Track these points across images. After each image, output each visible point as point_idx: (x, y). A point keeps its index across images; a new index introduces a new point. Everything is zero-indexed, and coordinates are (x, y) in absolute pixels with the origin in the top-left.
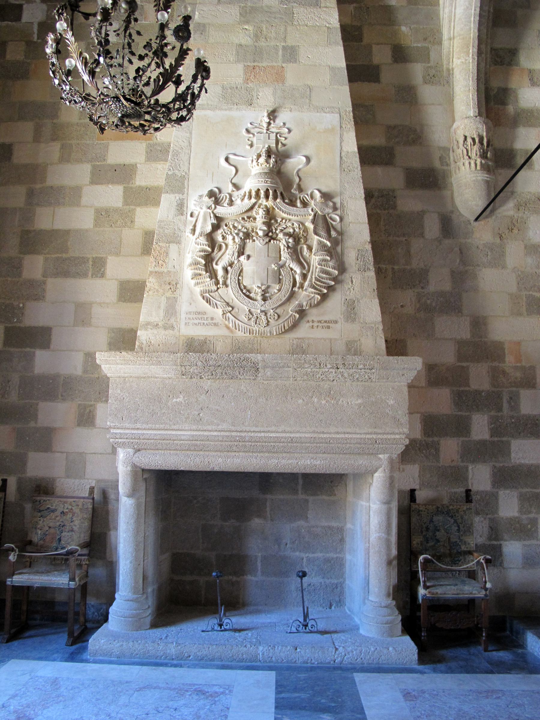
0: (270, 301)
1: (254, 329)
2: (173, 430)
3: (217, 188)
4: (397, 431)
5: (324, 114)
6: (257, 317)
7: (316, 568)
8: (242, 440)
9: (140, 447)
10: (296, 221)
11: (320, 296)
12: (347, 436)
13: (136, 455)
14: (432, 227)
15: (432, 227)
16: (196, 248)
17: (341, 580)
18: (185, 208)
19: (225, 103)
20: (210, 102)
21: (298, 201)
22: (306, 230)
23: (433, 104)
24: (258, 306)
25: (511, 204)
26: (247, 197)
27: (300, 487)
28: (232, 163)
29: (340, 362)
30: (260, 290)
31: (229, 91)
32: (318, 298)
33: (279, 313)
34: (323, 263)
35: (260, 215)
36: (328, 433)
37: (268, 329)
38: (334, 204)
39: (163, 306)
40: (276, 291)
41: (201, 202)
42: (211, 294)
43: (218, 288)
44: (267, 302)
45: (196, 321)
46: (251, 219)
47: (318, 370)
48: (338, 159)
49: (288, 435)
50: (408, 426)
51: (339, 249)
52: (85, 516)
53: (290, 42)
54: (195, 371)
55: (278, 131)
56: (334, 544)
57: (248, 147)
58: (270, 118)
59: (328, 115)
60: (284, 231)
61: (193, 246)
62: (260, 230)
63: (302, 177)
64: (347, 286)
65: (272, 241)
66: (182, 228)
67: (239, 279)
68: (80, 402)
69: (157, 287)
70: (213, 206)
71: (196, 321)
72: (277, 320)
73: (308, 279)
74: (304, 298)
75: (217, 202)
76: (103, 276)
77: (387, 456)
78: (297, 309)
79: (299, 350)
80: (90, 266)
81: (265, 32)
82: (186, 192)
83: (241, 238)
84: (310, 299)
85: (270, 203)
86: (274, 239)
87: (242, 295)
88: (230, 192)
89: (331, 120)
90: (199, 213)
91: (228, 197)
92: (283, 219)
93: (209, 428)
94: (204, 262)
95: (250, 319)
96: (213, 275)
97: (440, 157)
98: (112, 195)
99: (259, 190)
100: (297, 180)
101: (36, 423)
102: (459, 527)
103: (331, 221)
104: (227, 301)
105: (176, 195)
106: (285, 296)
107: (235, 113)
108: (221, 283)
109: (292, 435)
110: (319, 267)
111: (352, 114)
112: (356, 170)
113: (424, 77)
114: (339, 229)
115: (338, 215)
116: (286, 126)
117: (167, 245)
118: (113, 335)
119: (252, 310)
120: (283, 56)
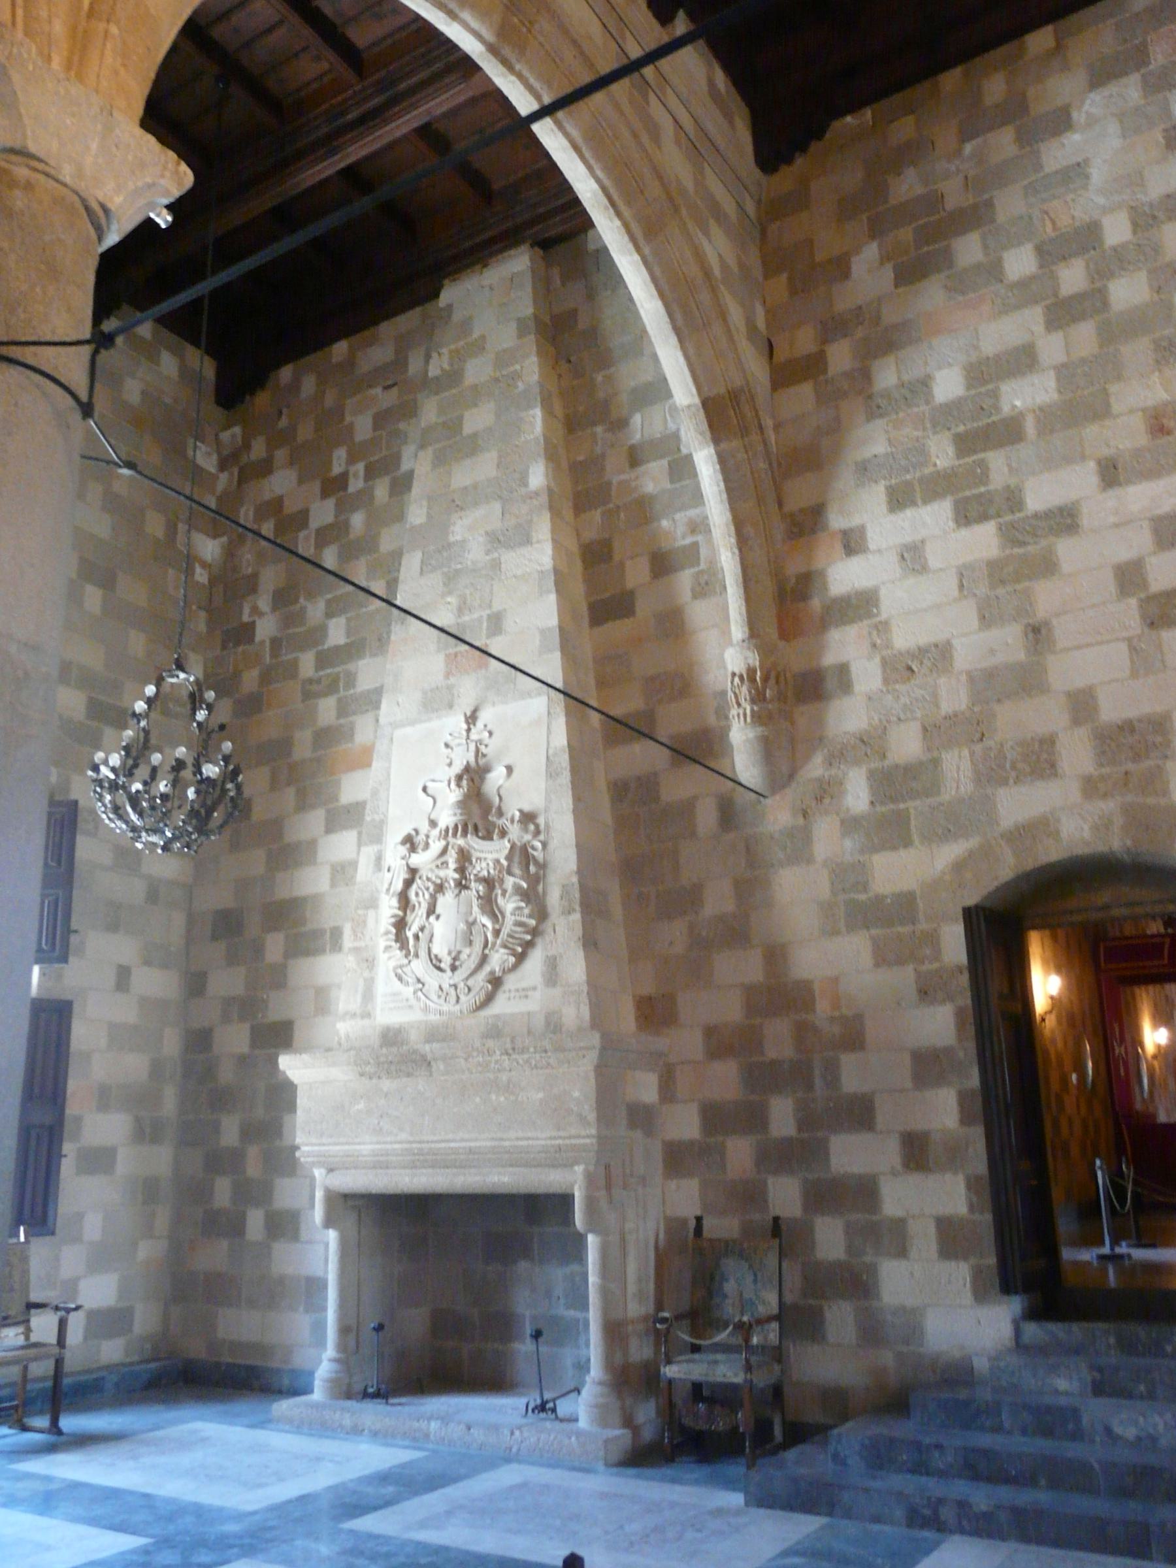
8: (421, 1152)
14: (707, 817)
15: (707, 817)
24: (447, 979)
25: (818, 759)
29: (509, 1046)
35: (452, 859)
37: (458, 1007)
44: (456, 973)
45: (392, 1005)
48: (544, 760)
51: (540, 888)
53: (496, 607)
64: (549, 936)
75: (413, 849)
79: (494, 1031)
81: (469, 601)
85: (461, 842)
95: (439, 997)
100: (497, 799)
102: (755, 1275)
107: (435, 724)
109: (472, 1144)
113: (693, 590)
120: (488, 629)
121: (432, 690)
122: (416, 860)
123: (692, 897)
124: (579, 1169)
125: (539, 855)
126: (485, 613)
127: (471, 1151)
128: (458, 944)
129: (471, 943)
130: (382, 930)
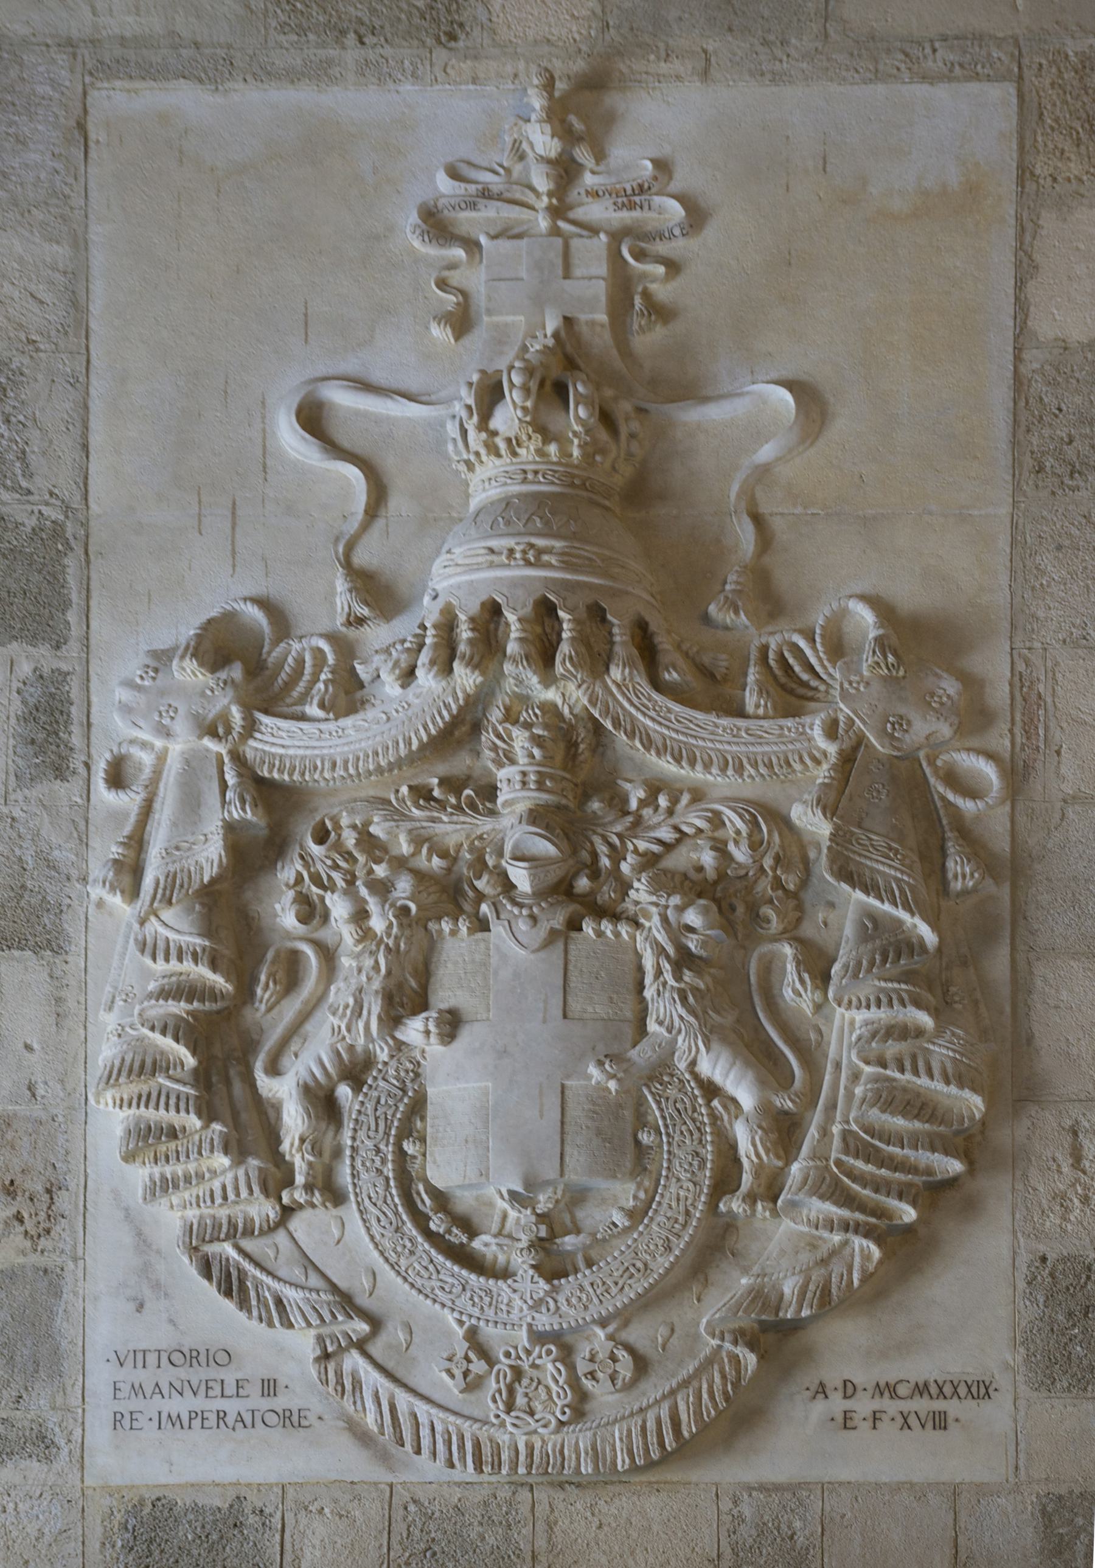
0: (585, 1276)
1: (503, 1439)
5: (921, 90)
11: (879, 1242)
18: (75, 729)
19: (283, 28)
22: (794, 852)
24: (517, 1308)
28: (345, 443)
32: (866, 1257)
34: (892, 1048)
37: (581, 1438)
38: (971, 683)
40: (619, 1218)
41: (162, 693)
42: (247, 1244)
43: (288, 1211)
46: (468, 792)
55: (626, 216)
57: (440, 333)
58: (566, 134)
59: (942, 92)
60: (671, 862)
61: (129, 960)
63: (778, 524)
65: (588, 928)
66: (64, 855)
67: (401, 1153)
70: (236, 715)
72: (630, 1386)
74: (783, 1253)
78: (746, 1321)
82: (76, 631)
83: (405, 910)
84: (824, 1262)
86: (601, 912)
90: (162, 757)
91: (331, 659)
94: (190, 1061)
95: (473, 1384)
96: (251, 1131)
100: (745, 535)
103: (951, 796)
104: (342, 1284)
106: (669, 1249)
107: (352, 101)
108: (300, 1179)
110: (868, 1069)
114: (1002, 844)
115: (990, 756)
116: (675, 186)
119: (489, 1332)
122: (281, 742)
125: (986, 809)
128: (576, 1159)
130: (107, 1052)
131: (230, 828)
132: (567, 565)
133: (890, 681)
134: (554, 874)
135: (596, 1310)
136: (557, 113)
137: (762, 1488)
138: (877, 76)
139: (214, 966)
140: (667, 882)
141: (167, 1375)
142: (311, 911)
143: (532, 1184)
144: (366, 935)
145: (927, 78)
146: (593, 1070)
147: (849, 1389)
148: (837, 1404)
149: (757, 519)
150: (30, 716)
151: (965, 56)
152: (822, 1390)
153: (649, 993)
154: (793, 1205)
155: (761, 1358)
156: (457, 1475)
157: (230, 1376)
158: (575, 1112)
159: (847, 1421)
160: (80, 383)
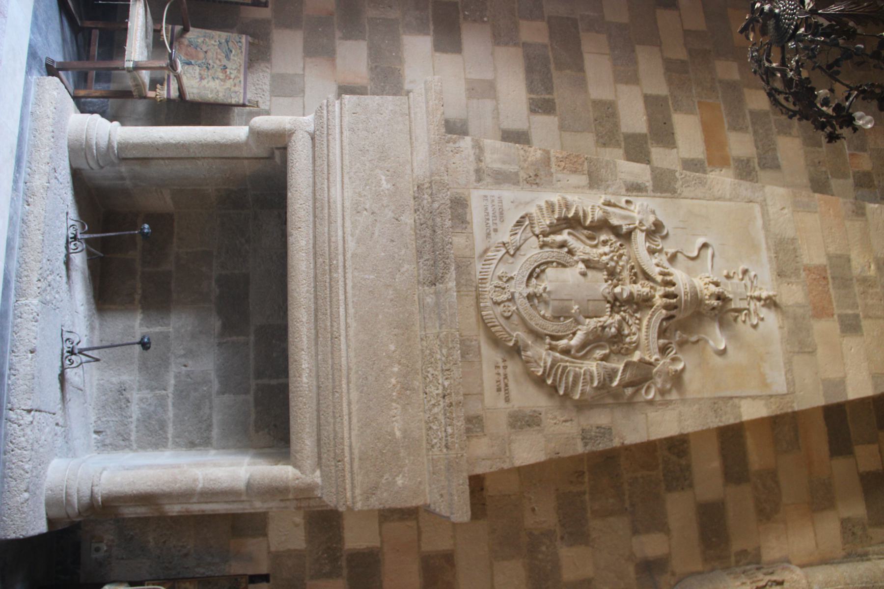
0: (528, 305)
1: (488, 285)
2: (342, 176)
3: (667, 234)
4: (358, 491)
5: (783, 373)
6: (504, 289)
7: (152, 408)
9: (317, 138)
10: (639, 338)
12: (346, 417)
13: (306, 134)
16: (587, 206)
17: (135, 446)
20: (772, 223)
21: (666, 341)
22: (629, 352)
23: (816, 535)
24: (520, 289)
26: (662, 269)
27: (266, 381)
28: (702, 252)
29: (454, 398)
30: (541, 291)
31: (792, 247)
33: (512, 318)
34: (588, 377)
35: (640, 288)
36: (348, 390)
38: (669, 391)
39: (505, 167)
40: (542, 313)
42: (529, 227)
43: (537, 236)
44: (526, 301)
45: (490, 210)
47: (439, 369)
48: (729, 394)
49: (343, 332)
50: (366, 508)
51: (610, 401)
52: (221, 95)
53: (865, 323)
54: (425, 202)
55: (752, 312)
56: (186, 434)
57: (725, 272)
59: (783, 378)
61: (590, 204)
62: (622, 289)
65: (608, 305)
66: (610, 190)
67: (553, 262)
68: (369, 88)
69: (529, 159)
70: (644, 228)
71: (490, 210)
73: (563, 357)
76: (533, 111)
77: (319, 480)
78: (520, 344)
80: (542, 96)
81: (871, 291)
84: (536, 361)
86: (612, 308)
87: (533, 267)
88: (665, 250)
89: (779, 383)
90: (633, 211)
92: (639, 319)
93: (348, 224)
94: (570, 215)
95: (500, 278)
96: (555, 229)
97: (746, 550)
98: (634, 118)
99: (674, 285)
100: (694, 338)
101: (341, 38)
105: (651, 182)
106: (537, 324)
107: (764, 255)
108: (545, 239)
109: (343, 339)
110: (582, 371)
111: (790, 410)
112: (717, 420)
114: (635, 400)
115: (654, 396)
117: (586, 172)
118: (459, 125)
119: (513, 282)
120: (847, 315)
121: (795, 250)
123: (576, 533)
124: (317, 477)
126: (860, 311)
127: (334, 338)
128: (556, 303)
129: (557, 318)
130: (570, 197)
131: (621, 226)
132: (685, 301)
133: (668, 373)
134: (619, 297)
135: (520, 308)
136: (769, 298)
137: (479, 347)
138: (785, 364)
139: (591, 222)
140: (620, 323)
141: (497, 208)
142: (605, 243)
143: (549, 293)
144: (601, 255)
145: (786, 374)
146: (576, 307)
147: (505, 367)
148: (501, 364)
149: (697, 341)
150: (638, 185)
151: (791, 383)
152: (504, 361)
153: (595, 319)
154: (549, 354)
155: (511, 347)
156: (478, 273)
157: (497, 221)
158: (566, 303)
159: (497, 367)
160: (704, 198)
